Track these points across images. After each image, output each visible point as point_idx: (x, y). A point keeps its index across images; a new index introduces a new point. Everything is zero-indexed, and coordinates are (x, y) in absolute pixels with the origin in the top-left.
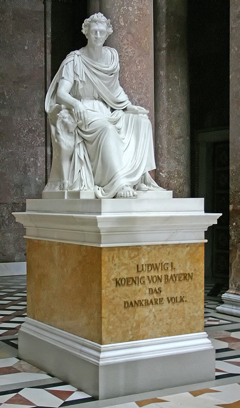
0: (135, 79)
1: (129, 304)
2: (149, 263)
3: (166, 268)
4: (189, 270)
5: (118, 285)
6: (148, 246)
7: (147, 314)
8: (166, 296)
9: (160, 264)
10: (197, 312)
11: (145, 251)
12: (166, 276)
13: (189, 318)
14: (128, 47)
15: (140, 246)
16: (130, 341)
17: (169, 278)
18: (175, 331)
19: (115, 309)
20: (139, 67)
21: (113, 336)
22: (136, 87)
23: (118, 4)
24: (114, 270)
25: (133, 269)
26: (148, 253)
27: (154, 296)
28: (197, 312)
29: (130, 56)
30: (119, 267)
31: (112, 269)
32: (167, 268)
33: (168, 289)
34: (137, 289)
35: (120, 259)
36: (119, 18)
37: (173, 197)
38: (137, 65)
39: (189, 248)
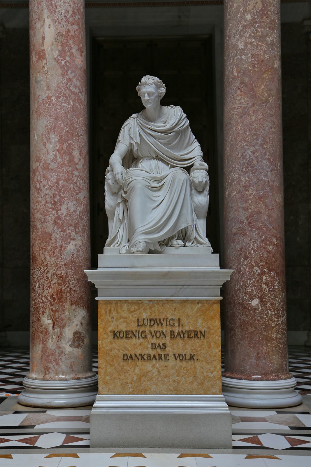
0: (249, 130)
1: (129, 358)
3: (172, 324)
4: (201, 327)
6: (150, 301)
7: (150, 368)
9: (164, 319)
10: (212, 372)
11: (146, 305)
12: (172, 333)
13: (202, 378)
15: (141, 300)
16: (130, 394)
17: (176, 334)
18: (184, 390)
19: (113, 360)
21: (111, 387)
22: (249, 139)
24: (111, 322)
25: (133, 322)
26: (151, 308)
27: (158, 351)
28: (212, 372)
30: (117, 320)
31: (108, 321)
32: (174, 324)
33: (175, 345)
34: (138, 343)
35: (118, 313)
36: (233, 69)
37: (213, 253)
38: (250, 116)
39: (200, 305)
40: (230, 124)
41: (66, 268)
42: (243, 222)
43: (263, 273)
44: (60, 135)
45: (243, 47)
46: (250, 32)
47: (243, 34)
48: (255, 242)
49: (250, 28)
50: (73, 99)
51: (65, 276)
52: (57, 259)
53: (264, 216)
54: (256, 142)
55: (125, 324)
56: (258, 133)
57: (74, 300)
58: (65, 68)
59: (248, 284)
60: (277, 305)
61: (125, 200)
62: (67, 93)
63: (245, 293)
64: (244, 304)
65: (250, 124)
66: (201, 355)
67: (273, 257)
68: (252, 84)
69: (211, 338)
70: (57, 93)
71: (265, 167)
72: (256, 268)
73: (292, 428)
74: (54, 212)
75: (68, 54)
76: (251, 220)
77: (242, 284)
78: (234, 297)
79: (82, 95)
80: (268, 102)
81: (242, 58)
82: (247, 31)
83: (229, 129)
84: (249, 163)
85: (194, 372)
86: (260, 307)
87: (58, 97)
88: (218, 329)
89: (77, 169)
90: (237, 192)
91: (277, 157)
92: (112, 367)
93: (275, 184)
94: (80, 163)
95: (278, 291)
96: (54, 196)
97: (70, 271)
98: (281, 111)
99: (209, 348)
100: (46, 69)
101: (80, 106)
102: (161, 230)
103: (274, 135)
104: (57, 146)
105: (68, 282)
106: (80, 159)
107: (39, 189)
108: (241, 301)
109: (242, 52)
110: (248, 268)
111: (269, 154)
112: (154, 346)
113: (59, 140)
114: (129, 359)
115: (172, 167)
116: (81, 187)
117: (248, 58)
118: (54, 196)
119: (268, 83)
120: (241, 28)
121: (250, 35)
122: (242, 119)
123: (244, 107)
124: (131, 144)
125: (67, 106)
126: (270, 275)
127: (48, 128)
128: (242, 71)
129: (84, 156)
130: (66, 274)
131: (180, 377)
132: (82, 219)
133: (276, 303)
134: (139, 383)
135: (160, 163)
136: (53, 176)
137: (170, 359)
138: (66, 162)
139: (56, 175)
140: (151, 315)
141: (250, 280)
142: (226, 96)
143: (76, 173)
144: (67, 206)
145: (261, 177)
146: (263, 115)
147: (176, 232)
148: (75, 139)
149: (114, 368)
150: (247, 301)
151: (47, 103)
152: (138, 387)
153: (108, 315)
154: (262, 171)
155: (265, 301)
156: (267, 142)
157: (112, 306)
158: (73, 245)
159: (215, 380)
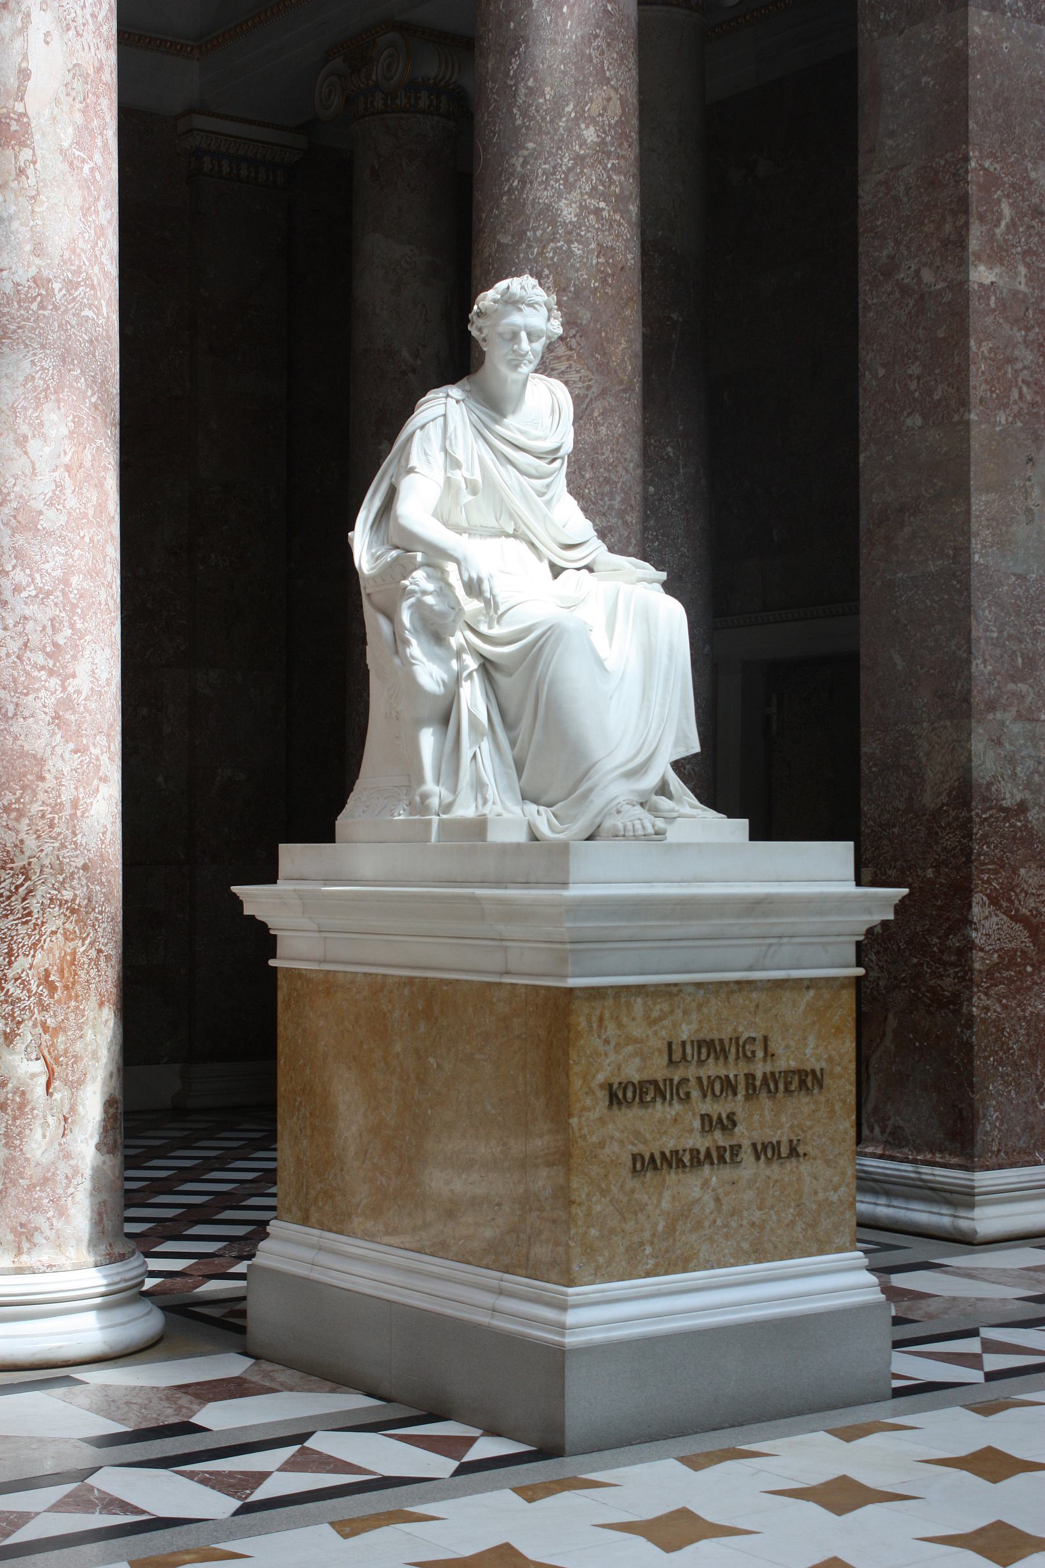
0: (592, 466)
1: (647, 1162)
2: (701, 1036)
3: (749, 1054)
4: (813, 1060)
6: (699, 985)
7: (697, 1192)
8: (750, 1138)
9: (731, 1039)
11: (689, 999)
12: (750, 1077)
13: (814, 1207)
14: (570, 367)
15: (676, 985)
16: (648, 1275)
17: (758, 1083)
18: (775, 1247)
20: (603, 430)
21: (601, 1259)
23: (539, 233)
24: (603, 1057)
25: (656, 1054)
27: (716, 1138)
30: (618, 1048)
32: (753, 1052)
33: (756, 1117)
34: (669, 1117)
35: (620, 1025)
39: (812, 993)
44: (74, 417)
45: (574, 219)
46: (594, 178)
47: (576, 181)
49: (592, 166)
52: (63, 846)
54: (608, 503)
55: (637, 1060)
56: (613, 477)
58: (92, 188)
61: (482, 660)
66: (813, 1140)
68: (599, 332)
69: (835, 1089)
74: (54, 682)
81: (570, 251)
82: (585, 174)
85: (796, 1192)
92: (605, 1197)
97: (98, 888)
99: (830, 1118)
100: (32, 181)
105: (94, 926)
113: (71, 433)
117: (588, 252)
118: (53, 625)
121: (594, 188)
127: (35, 388)
128: (572, 289)
130: (89, 900)
134: (671, 1241)
137: (745, 1157)
139: (60, 554)
140: (701, 1028)
149: (611, 1201)
151: (35, 298)
152: (667, 1251)
153: (596, 1035)
157: (606, 1004)
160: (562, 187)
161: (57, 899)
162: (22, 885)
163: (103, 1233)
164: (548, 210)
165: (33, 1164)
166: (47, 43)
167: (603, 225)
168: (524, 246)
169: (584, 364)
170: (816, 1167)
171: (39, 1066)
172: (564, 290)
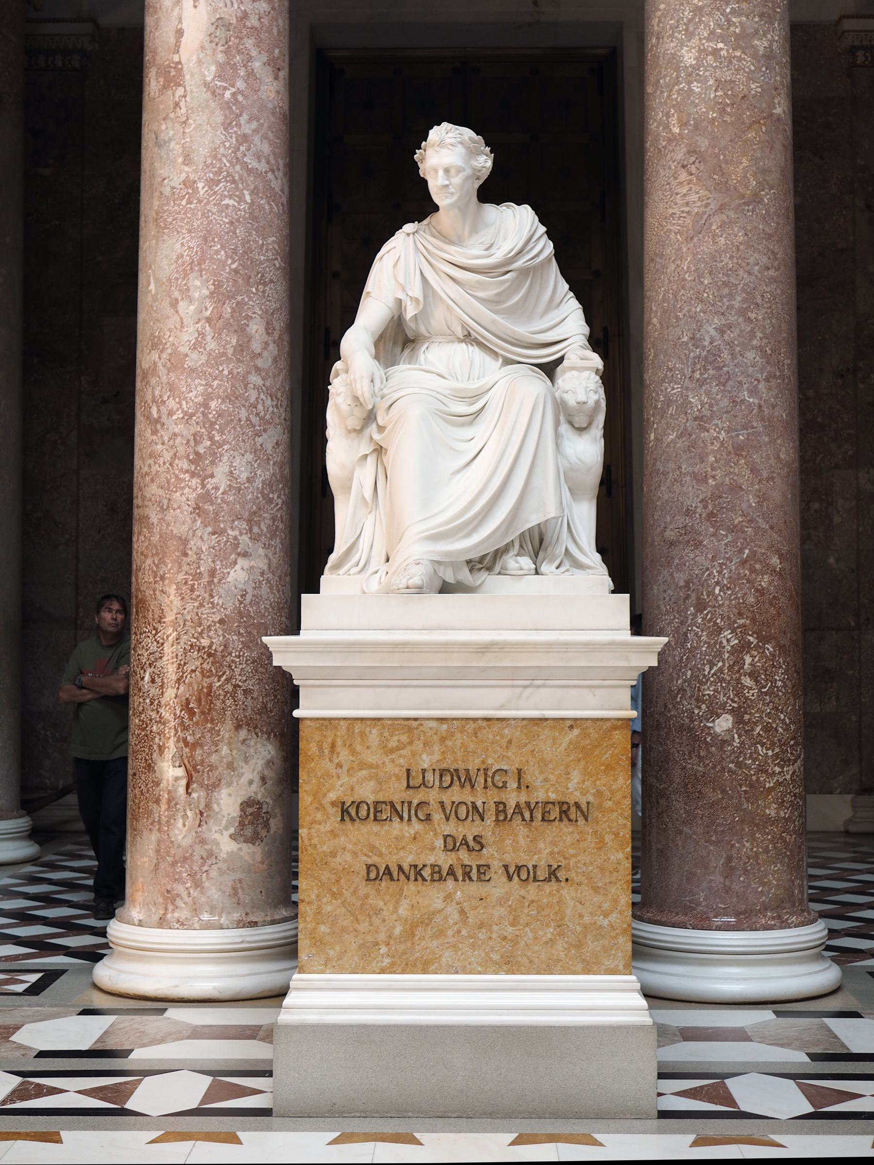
0: (710, 273)
2: (444, 766)
4: (578, 793)
5: (346, 818)
7: (438, 904)
8: (501, 860)
10: (606, 915)
12: (501, 807)
14: (690, 190)
15: (416, 719)
16: (383, 971)
18: (531, 962)
20: (722, 240)
21: (331, 952)
22: (711, 296)
24: (335, 779)
25: (394, 779)
26: (443, 739)
28: (606, 915)
29: (693, 213)
31: (328, 775)
32: (505, 783)
33: (508, 842)
34: (407, 835)
35: (353, 752)
36: (668, 115)
37: (613, 592)
38: (715, 236)
39: (576, 732)
40: (662, 255)
41: (224, 631)
42: (695, 513)
43: (744, 647)
44: (215, 281)
45: (694, 62)
46: (712, 24)
47: (695, 29)
48: (725, 564)
49: (710, 14)
50: (252, 187)
51: (222, 651)
52: (201, 605)
53: (747, 497)
54: (727, 303)
55: (372, 783)
56: (733, 280)
57: (245, 717)
58: (234, 108)
59: (704, 676)
60: (780, 729)
61: (379, 448)
62: (237, 172)
63: (697, 700)
64: (694, 728)
65: (713, 258)
66: (577, 867)
67: (771, 604)
68: (717, 156)
69: (605, 822)
70: (210, 172)
71: (751, 369)
72: (727, 633)
73: (814, 1057)
74: (195, 482)
75: (242, 73)
76: (715, 506)
77: (689, 677)
78: (669, 711)
79: (277, 178)
80: (759, 202)
81: (691, 90)
82: (704, 22)
83: (657, 270)
84: (711, 359)
85: (557, 913)
86: (736, 736)
87: (212, 183)
88: (624, 797)
89: (258, 369)
90: (680, 432)
91: (783, 343)
92: (336, 900)
93: (776, 414)
94: (265, 354)
95: (784, 694)
96: (197, 438)
97: (235, 638)
98: (793, 225)
99: (600, 849)
100: (183, 111)
101: (271, 205)
102: (475, 529)
103: (773, 286)
104: (206, 309)
105: (230, 666)
106: (267, 344)
107: (157, 421)
108: (687, 721)
109: (692, 74)
110: (705, 633)
111: (761, 335)
112: (451, 844)
113: (212, 293)
114: (381, 880)
115: (508, 362)
116: (268, 417)
117: (706, 88)
118: (195, 439)
119: (758, 154)
120: (688, 14)
121: (712, 33)
122: (692, 245)
123: (697, 213)
124: (399, 302)
125: (236, 204)
126: (764, 652)
127: (184, 263)
128: (692, 122)
129: (276, 335)
130: (225, 646)
131: (521, 927)
132: (270, 501)
133: (777, 724)
134: (409, 944)
135: (475, 352)
136: (193, 386)
138: (230, 351)
139: (201, 385)
140: (445, 758)
141: (712, 664)
142: (649, 186)
143: (255, 379)
144: (231, 466)
145: (740, 394)
146: (746, 234)
147: (514, 535)
148: (254, 290)
149: (342, 903)
150: (701, 721)
151: (184, 197)
152: (404, 953)
154: (744, 380)
155: (749, 720)
156: (757, 304)
158: (243, 569)
159: (613, 934)
160: (683, 37)
161: (196, 646)
162: (170, 635)
163: (238, 904)
164: (674, 58)
165: (176, 846)
166: (195, 7)
167: (721, 63)
168: (659, 92)
169: (703, 185)
170: (581, 893)
171: (180, 772)
172: (686, 124)
